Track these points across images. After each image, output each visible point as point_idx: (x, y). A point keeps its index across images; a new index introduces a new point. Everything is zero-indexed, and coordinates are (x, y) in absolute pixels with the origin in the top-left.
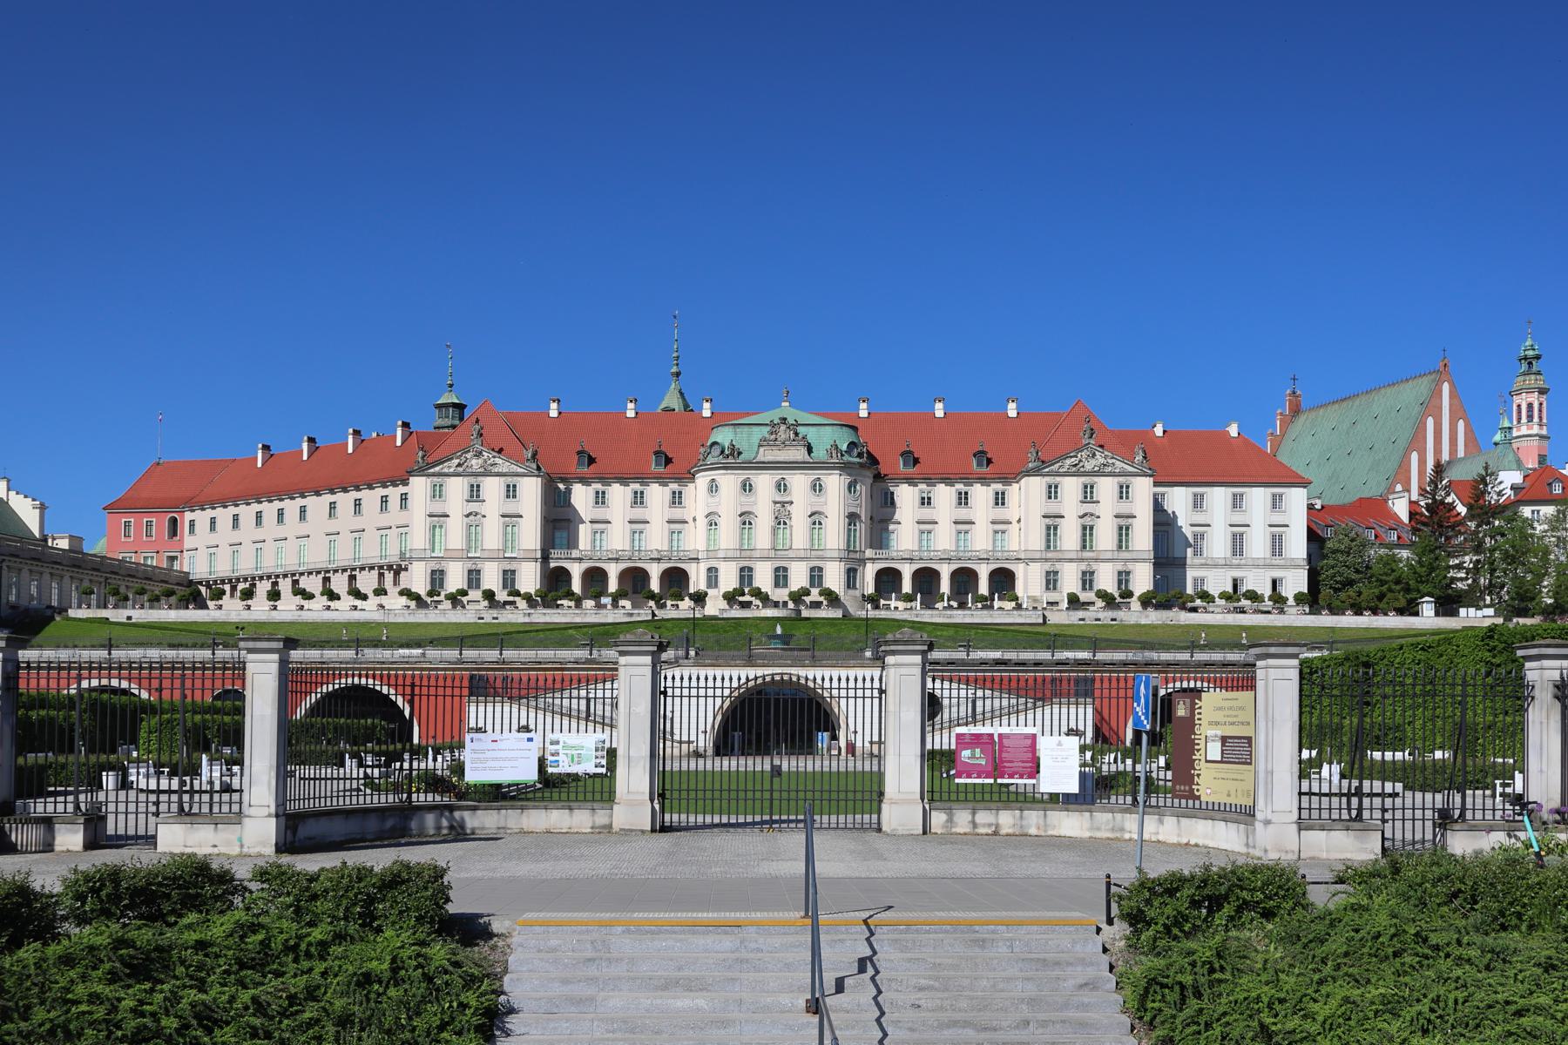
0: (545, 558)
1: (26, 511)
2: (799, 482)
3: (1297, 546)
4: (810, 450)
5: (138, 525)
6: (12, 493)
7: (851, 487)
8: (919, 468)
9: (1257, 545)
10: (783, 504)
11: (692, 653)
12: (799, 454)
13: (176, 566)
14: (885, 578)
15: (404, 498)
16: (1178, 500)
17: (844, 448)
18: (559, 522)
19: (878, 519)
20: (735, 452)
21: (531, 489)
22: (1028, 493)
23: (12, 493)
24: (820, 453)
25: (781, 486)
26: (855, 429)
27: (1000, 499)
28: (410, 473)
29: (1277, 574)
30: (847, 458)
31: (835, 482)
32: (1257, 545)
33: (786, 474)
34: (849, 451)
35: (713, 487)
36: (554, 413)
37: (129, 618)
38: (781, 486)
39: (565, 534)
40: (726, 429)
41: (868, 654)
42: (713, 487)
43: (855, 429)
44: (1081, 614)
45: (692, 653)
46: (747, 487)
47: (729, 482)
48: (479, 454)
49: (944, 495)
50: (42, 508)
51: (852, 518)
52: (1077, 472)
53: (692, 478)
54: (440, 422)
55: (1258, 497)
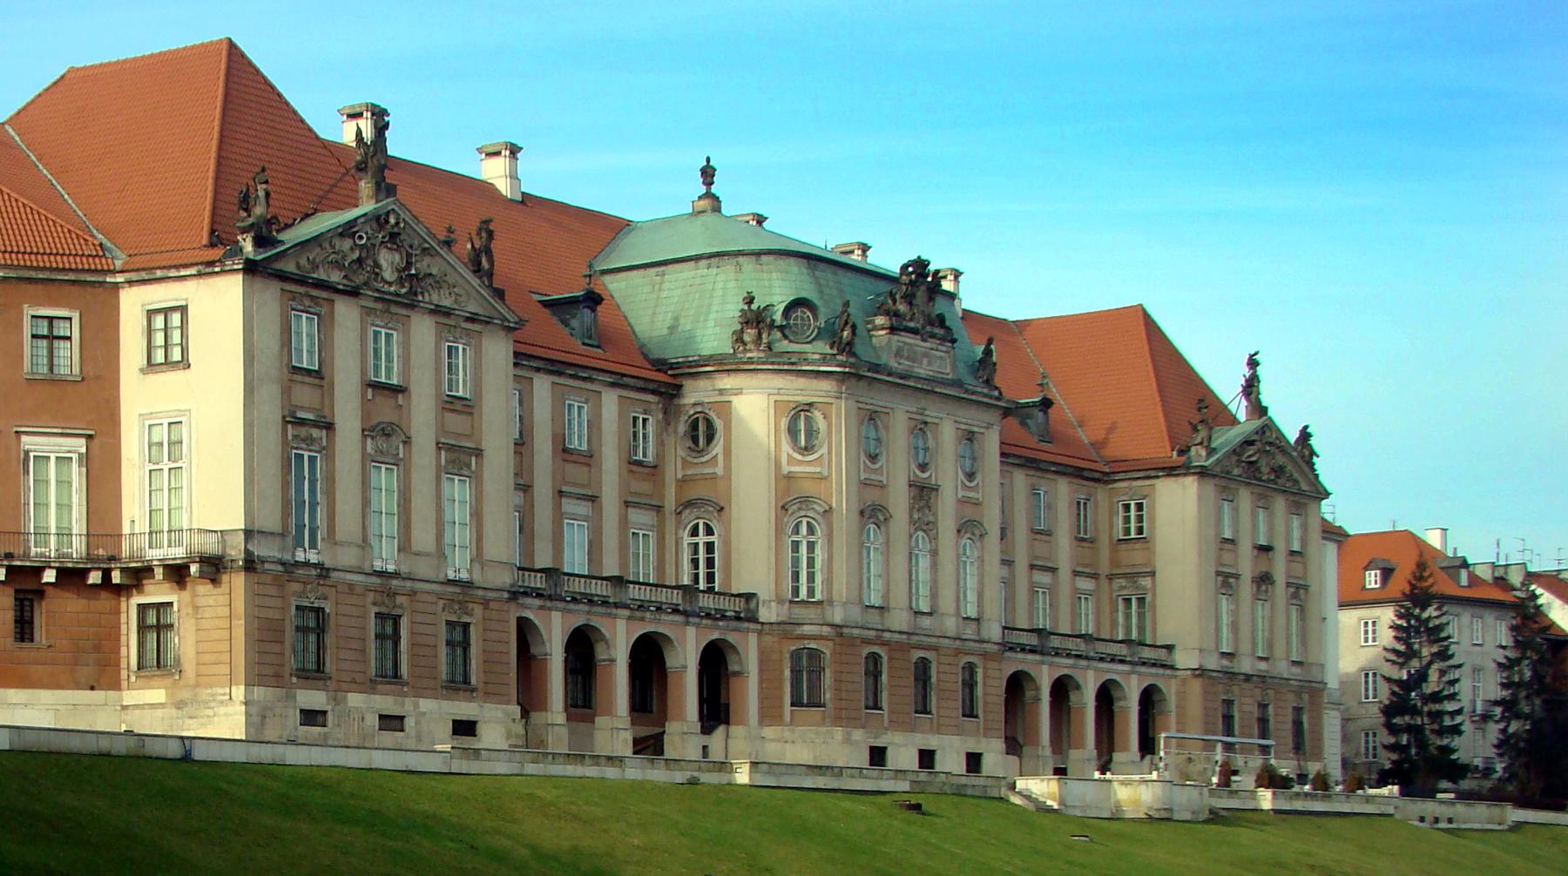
33: (933, 411)
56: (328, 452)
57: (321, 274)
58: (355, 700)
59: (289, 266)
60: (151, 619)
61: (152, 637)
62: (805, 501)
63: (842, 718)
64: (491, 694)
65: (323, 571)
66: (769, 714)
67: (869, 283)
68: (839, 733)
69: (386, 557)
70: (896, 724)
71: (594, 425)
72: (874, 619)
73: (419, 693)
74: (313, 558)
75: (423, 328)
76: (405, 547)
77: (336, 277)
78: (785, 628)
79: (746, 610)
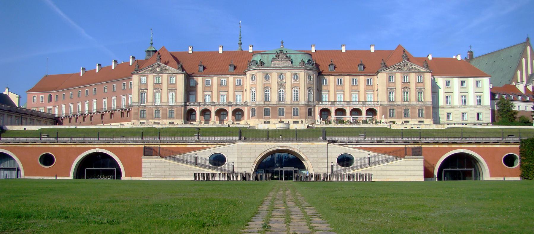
0: (185, 106)
1: (14, 99)
2: (288, 74)
3: (486, 100)
4: (292, 62)
5: (38, 98)
6: (10, 93)
7: (309, 76)
8: (336, 70)
9: (471, 101)
10: (282, 83)
11: (243, 138)
12: (288, 64)
13: (51, 112)
14: (323, 113)
15: (131, 84)
16: (440, 81)
17: (306, 62)
18: (190, 90)
19: (319, 90)
20: (262, 63)
21: (180, 79)
22: (381, 79)
23: (10, 93)
24: (297, 63)
25: (281, 77)
26: (310, 55)
27: (369, 82)
28: (133, 74)
29: (479, 111)
30: (307, 65)
31: (303, 74)
32: (471, 101)
34: (308, 63)
35: (253, 78)
36: (190, 52)
37: (25, 129)
38: (281, 77)
39: (194, 96)
40: (258, 55)
41: (321, 138)
42: (253, 78)
43: (310, 55)
44: (405, 126)
45: (243, 138)
46: (267, 77)
47: (259, 75)
48: (159, 66)
49: (347, 80)
50: (20, 97)
51: (309, 88)
52: (400, 70)
53: (244, 74)
54: (148, 57)
55: (471, 81)
56: (147, 92)
57: (146, 73)
58: (150, 120)
59: (141, 72)
60: (170, 112)
61: (170, 114)
62: (252, 88)
63: (260, 117)
64: (178, 118)
65: (145, 106)
66: (248, 118)
67: (270, 55)
68: (257, 120)
69: (158, 103)
70: (273, 118)
71: (228, 81)
72: (268, 103)
73: (163, 118)
74: (144, 105)
75: (165, 76)
76: (161, 102)
77: (149, 72)
78: (250, 106)
79: (246, 104)
